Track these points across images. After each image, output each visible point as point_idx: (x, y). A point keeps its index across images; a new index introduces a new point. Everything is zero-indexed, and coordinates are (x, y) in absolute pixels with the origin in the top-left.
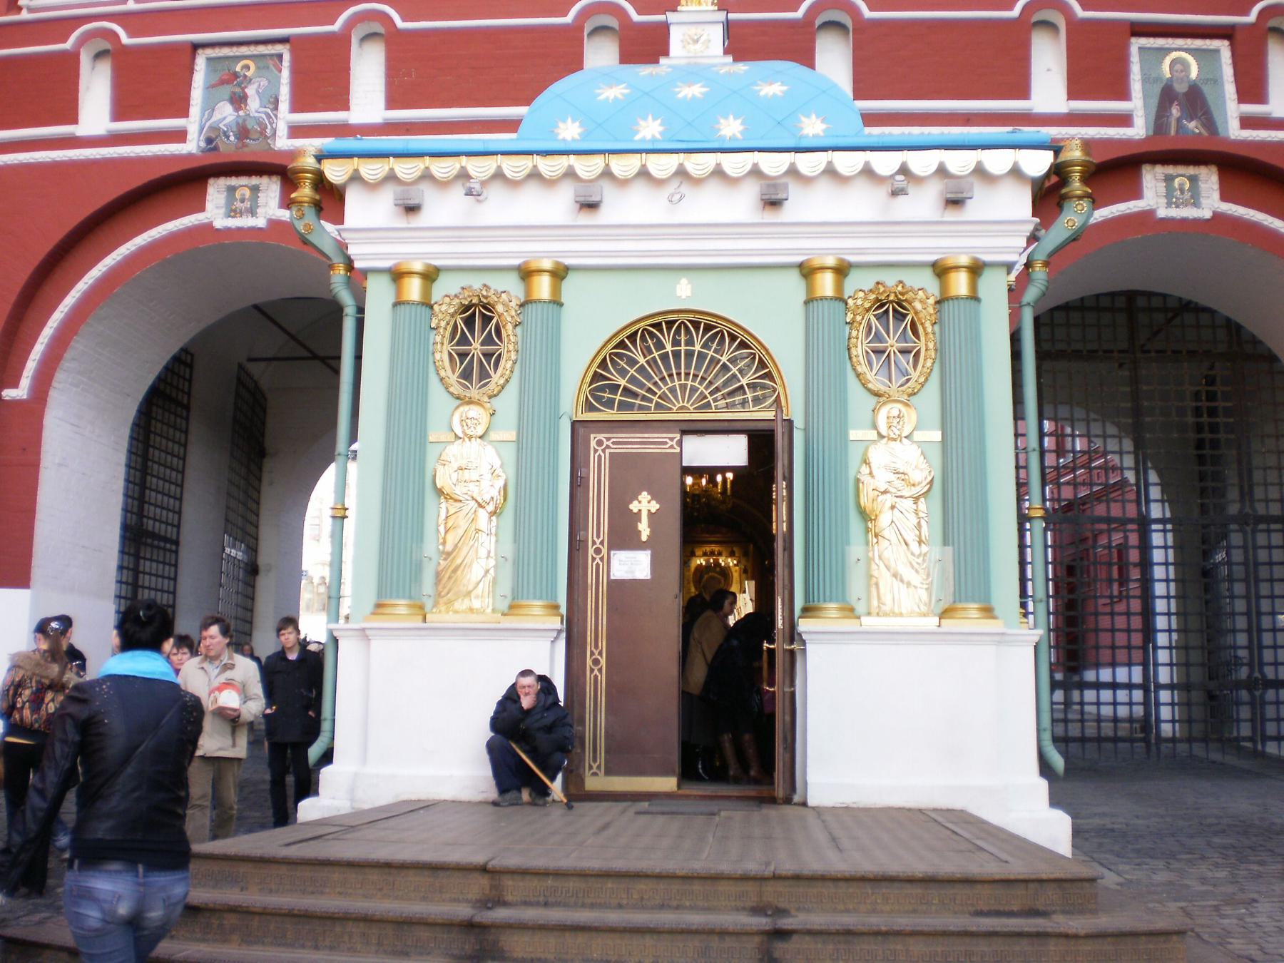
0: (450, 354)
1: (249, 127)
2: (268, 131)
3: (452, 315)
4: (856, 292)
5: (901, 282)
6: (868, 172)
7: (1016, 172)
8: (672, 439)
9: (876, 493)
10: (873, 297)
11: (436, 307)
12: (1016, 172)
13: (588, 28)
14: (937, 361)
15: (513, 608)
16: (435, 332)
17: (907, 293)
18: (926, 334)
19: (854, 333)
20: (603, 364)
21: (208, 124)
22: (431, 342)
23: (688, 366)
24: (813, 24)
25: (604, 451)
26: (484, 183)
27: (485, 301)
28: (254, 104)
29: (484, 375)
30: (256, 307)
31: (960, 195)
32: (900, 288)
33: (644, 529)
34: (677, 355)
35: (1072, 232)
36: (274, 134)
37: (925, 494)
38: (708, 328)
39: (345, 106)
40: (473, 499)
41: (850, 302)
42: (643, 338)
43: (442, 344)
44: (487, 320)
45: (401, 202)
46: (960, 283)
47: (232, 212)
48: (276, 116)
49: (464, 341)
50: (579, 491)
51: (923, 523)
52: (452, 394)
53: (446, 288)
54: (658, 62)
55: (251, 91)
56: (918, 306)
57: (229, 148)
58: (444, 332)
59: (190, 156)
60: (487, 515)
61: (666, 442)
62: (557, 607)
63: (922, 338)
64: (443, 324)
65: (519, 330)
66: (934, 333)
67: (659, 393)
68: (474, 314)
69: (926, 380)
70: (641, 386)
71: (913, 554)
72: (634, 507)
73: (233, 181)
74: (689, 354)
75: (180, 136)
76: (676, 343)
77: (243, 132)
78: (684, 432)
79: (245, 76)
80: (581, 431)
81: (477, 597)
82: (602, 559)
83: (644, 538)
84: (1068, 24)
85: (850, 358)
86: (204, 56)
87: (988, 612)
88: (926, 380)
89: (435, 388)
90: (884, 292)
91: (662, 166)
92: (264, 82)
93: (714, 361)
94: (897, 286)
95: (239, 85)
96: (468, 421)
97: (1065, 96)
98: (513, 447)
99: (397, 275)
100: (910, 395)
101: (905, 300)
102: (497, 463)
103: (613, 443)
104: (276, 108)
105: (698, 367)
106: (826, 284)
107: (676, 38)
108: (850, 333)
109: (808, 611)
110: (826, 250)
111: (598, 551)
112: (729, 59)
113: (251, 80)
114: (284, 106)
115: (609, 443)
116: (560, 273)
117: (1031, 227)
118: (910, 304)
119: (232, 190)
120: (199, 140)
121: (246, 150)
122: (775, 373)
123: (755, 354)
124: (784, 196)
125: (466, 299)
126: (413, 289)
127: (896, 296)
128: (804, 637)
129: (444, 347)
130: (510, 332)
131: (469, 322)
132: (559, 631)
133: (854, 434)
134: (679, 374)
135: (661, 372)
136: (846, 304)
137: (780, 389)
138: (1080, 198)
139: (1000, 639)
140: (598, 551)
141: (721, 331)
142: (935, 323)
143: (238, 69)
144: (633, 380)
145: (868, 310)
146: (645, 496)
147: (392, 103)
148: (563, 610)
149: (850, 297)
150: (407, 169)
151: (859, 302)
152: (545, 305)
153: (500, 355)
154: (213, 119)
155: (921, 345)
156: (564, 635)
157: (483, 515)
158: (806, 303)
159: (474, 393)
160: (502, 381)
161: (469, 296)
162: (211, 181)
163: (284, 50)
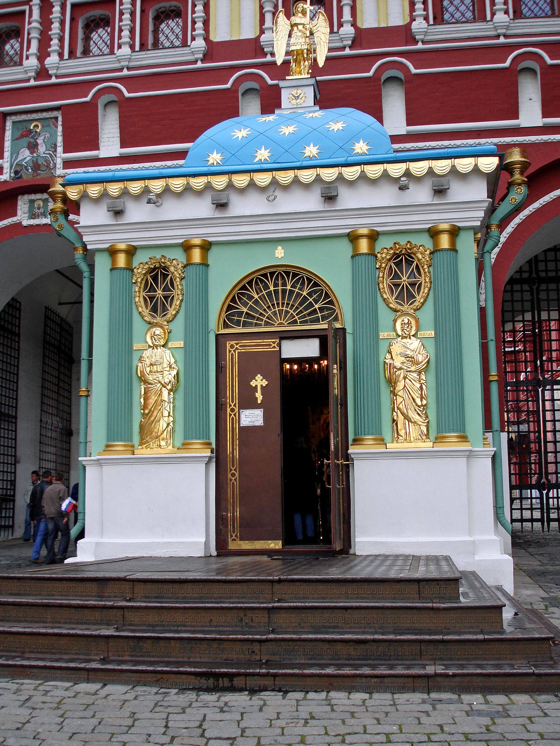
0: (145, 299)
1: (40, 163)
2: (51, 165)
3: (145, 274)
4: (382, 249)
5: (409, 242)
6: (385, 175)
7: (476, 170)
8: (274, 343)
9: (395, 370)
10: (392, 252)
11: (135, 270)
12: (476, 170)
13: (241, 90)
14: (432, 289)
15: (185, 446)
16: (135, 285)
17: (413, 248)
18: (425, 273)
19: (381, 275)
20: (233, 300)
21: (15, 163)
22: (134, 290)
23: (283, 298)
24: (380, 80)
25: (234, 351)
26: (159, 196)
27: (163, 265)
28: (42, 149)
29: (164, 309)
30: (57, 271)
31: (441, 188)
32: (408, 246)
33: (259, 396)
34: (276, 292)
35: (514, 206)
36: (55, 167)
37: (426, 370)
38: (295, 275)
39: (98, 149)
40: (160, 382)
41: (379, 255)
42: (257, 283)
43: (139, 292)
44: (165, 276)
45: (110, 209)
46: (445, 241)
47: (33, 216)
48: (56, 156)
49: (152, 289)
50: (221, 375)
51: (424, 387)
52: (146, 321)
53: (141, 258)
54: (274, 113)
55: (40, 141)
56: (420, 256)
57: (28, 176)
58: (141, 285)
59: (6, 181)
60: (167, 391)
61: (271, 345)
62: (209, 444)
63: (423, 275)
64: (139, 280)
65: (184, 282)
66: (429, 272)
67: (267, 315)
68: (157, 273)
69: (425, 300)
70: (257, 311)
71: (417, 405)
72: (253, 383)
73: (33, 197)
74: (284, 291)
76: (276, 285)
77: (36, 166)
78: (282, 338)
79: (36, 132)
80: (221, 339)
81: (163, 439)
82: (235, 415)
83: (259, 402)
84: (541, 69)
85: (379, 289)
86: (11, 121)
87: (464, 438)
88: (425, 300)
89: (136, 317)
90: (399, 248)
91: (263, 179)
92: (48, 135)
93: (299, 295)
94: (407, 245)
95: (33, 137)
96: (155, 337)
97: (540, 115)
98: (182, 351)
99: (112, 252)
100: (415, 310)
101: (412, 253)
102: (173, 360)
103: (240, 346)
104: (56, 151)
105: (289, 299)
106: (364, 245)
107: (285, 95)
108: (379, 274)
109: (356, 441)
111: (233, 410)
112: (317, 108)
113: (40, 134)
114: (60, 149)
115: (237, 346)
116: (206, 247)
117: (486, 204)
118: (415, 255)
119: (32, 202)
120: (10, 173)
121: (38, 177)
122: (334, 300)
123: (322, 290)
124: (335, 194)
125: (152, 264)
126: (121, 260)
127: (406, 250)
128: (352, 456)
129: (141, 294)
130: (178, 283)
131: (155, 278)
132: (210, 458)
133: (383, 335)
134: (278, 304)
135: (268, 303)
136: (376, 257)
137: (337, 311)
138: (519, 184)
139: (470, 455)
140: (233, 410)
141: (303, 277)
142: (430, 266)
143: (32, 128)
144: (251, 308)
145: (389, 260)
146: (259, 377)
147: (123, 144)
148: (214, 446)
149: (378, 253)
150: (114, 189)
151: (384, 255)
152: (198, 266)
153: (173, 296)
154: (19, 159)
155: (422, 279)
156: (214, 460)
157: (165, 392)
158: (352, 257)
159: (158, 320)
160: (174, 312)
161: (154, 263)
162: (20, 197)
163: (58, 114)
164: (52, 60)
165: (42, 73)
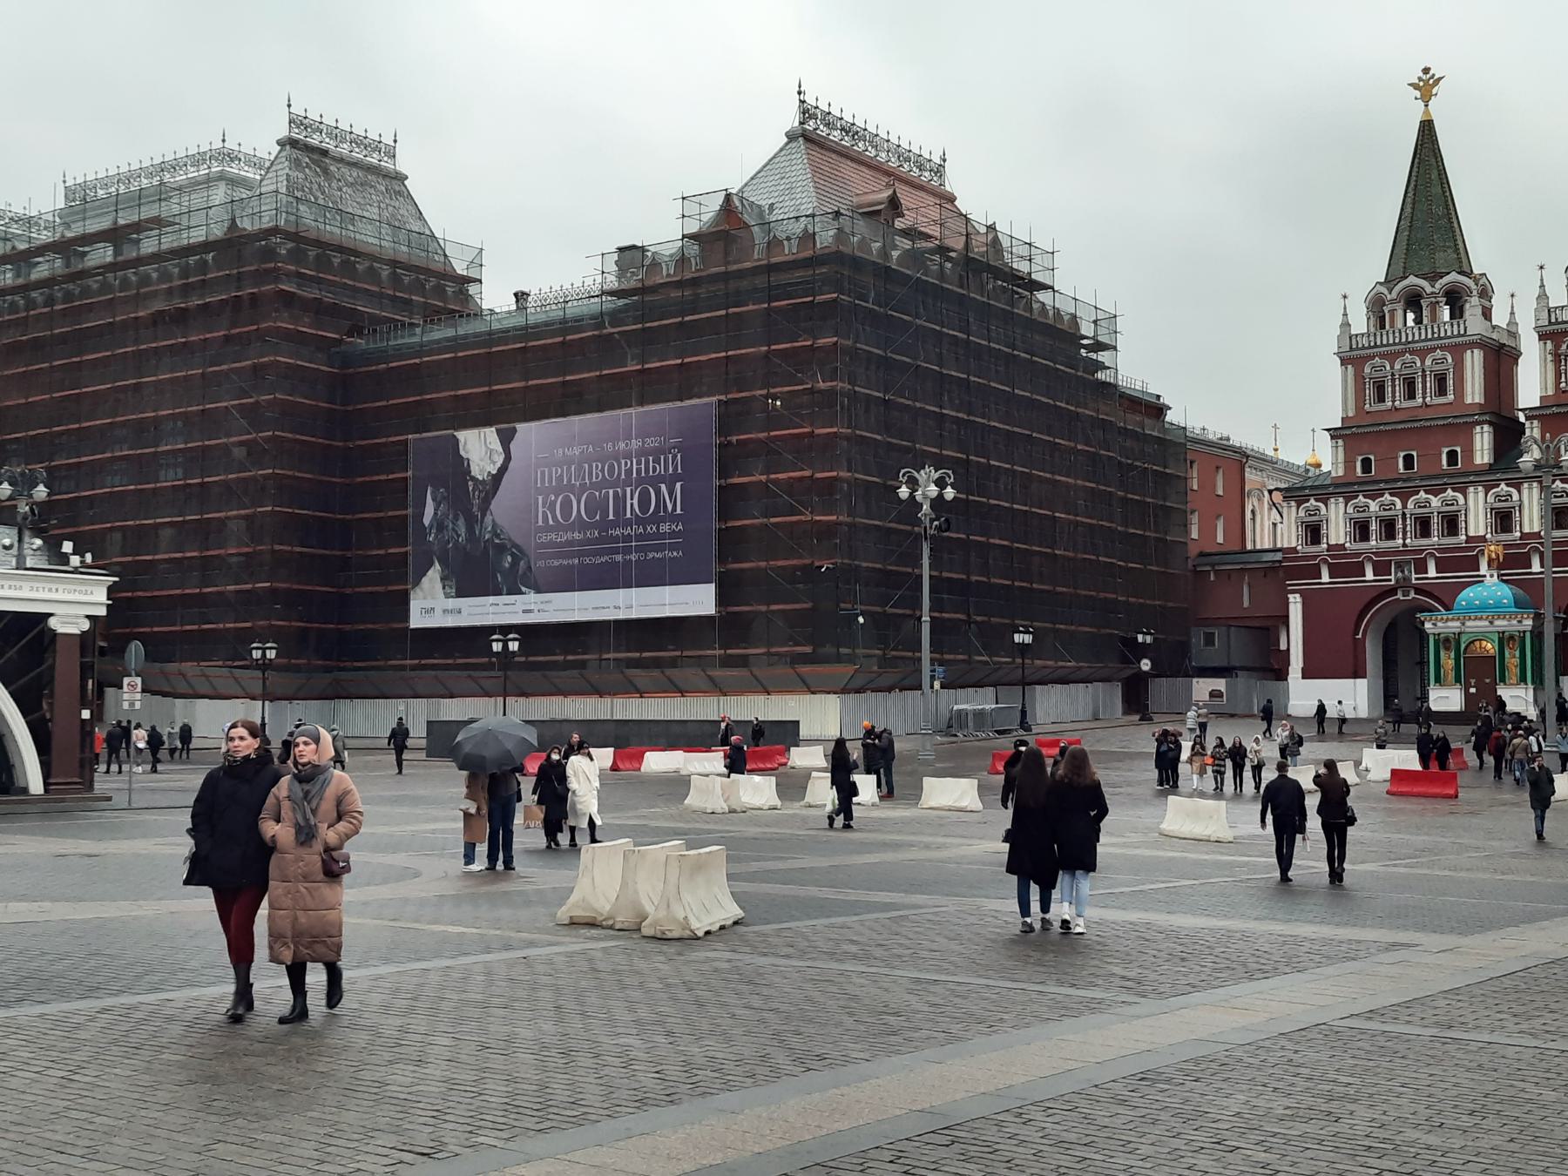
28: (1406, 572)
75: (1390, 580)
110: (1500, 629)
116: (1459, 634)
164: (1408, 541)
165: (1404, 545)
